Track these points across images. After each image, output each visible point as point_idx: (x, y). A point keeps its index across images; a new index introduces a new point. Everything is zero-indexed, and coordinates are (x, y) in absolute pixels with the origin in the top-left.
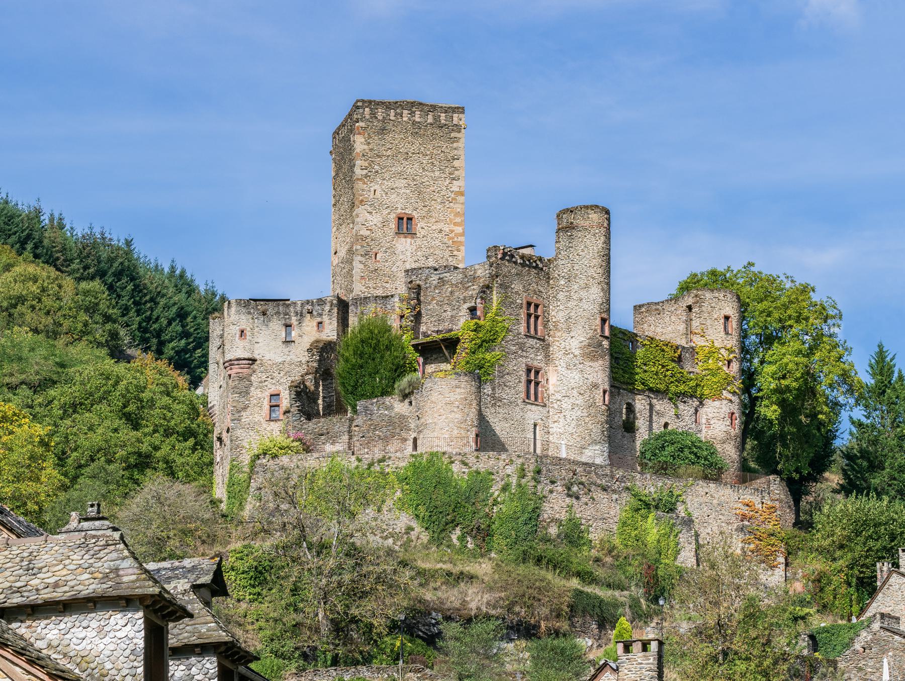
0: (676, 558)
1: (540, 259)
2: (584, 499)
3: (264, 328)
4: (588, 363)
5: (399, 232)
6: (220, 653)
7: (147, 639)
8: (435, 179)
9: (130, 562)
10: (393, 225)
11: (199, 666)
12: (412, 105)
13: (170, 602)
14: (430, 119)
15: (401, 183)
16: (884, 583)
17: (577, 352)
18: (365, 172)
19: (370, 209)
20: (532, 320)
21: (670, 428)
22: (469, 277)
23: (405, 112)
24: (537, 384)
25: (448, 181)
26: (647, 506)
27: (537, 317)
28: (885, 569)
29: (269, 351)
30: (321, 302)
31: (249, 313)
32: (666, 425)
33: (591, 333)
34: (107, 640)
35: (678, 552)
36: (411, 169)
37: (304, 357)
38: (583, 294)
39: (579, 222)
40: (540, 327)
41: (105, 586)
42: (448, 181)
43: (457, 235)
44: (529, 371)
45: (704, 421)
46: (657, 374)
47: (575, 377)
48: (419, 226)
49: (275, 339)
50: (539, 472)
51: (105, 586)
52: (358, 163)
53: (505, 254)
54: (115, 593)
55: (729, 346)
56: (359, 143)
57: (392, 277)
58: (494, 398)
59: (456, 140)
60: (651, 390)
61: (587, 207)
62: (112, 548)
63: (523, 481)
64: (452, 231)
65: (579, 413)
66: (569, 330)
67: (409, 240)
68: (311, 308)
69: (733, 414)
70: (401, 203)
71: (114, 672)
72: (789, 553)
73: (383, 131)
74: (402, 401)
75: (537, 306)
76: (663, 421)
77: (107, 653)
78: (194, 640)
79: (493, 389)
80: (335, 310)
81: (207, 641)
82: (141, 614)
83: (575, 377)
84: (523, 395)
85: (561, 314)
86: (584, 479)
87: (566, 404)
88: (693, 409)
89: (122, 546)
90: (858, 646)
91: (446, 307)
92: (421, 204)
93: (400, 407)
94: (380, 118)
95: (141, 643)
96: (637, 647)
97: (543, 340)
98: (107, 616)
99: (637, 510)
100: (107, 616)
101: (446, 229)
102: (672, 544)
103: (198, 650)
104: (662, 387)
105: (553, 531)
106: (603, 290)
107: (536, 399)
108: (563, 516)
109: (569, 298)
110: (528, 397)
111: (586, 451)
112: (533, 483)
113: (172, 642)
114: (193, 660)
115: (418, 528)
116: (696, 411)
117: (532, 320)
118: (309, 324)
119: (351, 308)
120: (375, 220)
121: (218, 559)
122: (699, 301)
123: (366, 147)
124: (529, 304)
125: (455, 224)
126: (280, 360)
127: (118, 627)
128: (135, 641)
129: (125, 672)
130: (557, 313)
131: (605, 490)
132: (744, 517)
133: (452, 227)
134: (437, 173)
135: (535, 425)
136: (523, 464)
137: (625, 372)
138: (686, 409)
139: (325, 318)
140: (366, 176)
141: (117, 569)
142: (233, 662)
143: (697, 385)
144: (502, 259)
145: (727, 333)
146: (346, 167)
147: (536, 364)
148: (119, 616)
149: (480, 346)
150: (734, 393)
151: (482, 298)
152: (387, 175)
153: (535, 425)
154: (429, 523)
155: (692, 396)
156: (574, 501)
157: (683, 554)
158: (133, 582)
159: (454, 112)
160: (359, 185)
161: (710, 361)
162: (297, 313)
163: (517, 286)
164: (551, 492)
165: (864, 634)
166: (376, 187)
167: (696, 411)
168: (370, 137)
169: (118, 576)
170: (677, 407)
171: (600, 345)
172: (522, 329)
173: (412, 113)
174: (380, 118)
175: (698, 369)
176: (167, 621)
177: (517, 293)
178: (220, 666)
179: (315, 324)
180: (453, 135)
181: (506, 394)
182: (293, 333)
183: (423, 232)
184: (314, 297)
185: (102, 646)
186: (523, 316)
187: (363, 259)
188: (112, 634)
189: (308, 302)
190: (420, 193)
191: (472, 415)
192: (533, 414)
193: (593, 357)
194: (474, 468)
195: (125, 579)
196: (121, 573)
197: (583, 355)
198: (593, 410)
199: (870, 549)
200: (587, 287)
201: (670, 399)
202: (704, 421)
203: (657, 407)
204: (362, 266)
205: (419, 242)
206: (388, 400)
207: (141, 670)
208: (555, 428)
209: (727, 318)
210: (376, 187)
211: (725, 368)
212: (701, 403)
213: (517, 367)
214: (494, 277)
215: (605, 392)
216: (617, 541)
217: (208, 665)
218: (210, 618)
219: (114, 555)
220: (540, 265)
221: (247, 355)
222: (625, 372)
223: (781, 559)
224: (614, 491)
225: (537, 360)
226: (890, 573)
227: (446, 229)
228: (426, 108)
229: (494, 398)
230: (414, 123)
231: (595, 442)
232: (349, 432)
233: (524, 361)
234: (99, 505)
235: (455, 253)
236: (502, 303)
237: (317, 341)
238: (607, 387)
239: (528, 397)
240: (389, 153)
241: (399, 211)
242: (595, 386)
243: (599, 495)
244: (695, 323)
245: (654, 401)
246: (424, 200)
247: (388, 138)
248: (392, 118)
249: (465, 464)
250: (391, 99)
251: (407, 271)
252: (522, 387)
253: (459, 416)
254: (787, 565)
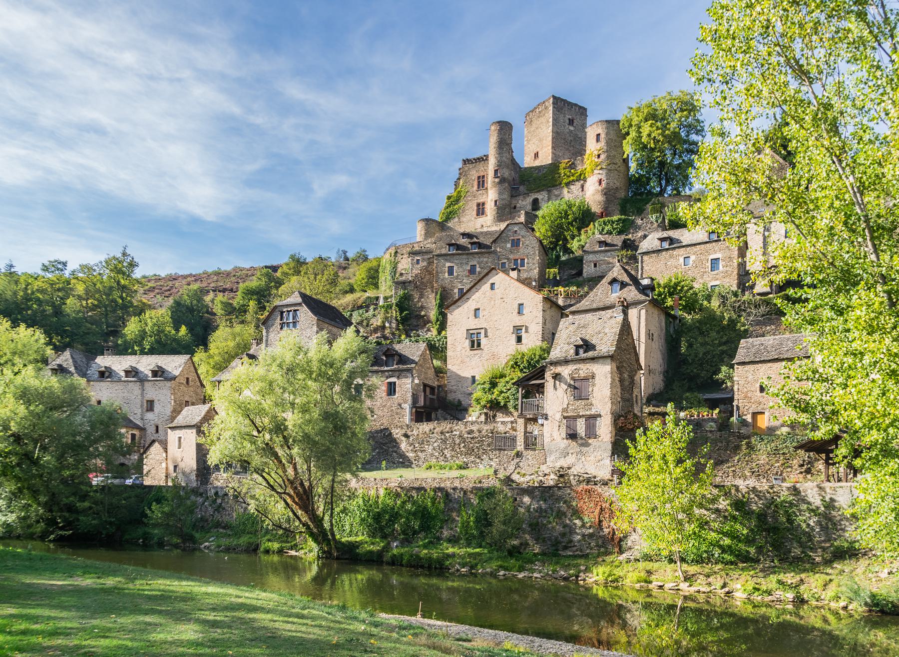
24: (483, 209)
27: (483, 181)
44: (478, 205)
55: (599, 148)
69: (601, 180)
75: (483, 177)
110: (477, 215)
116: (582, 187)
124: (479, 177)
138: (575, 188)
143: (581, 175)
150: (601, 169)
155: (577, 180)
186: (476, 183)
209: (598, 135)
211: (596, 160)
212: (585, 181)
214: (460, 174)
215: (496, 201)
236: (465, 182)
252: (475, 213)
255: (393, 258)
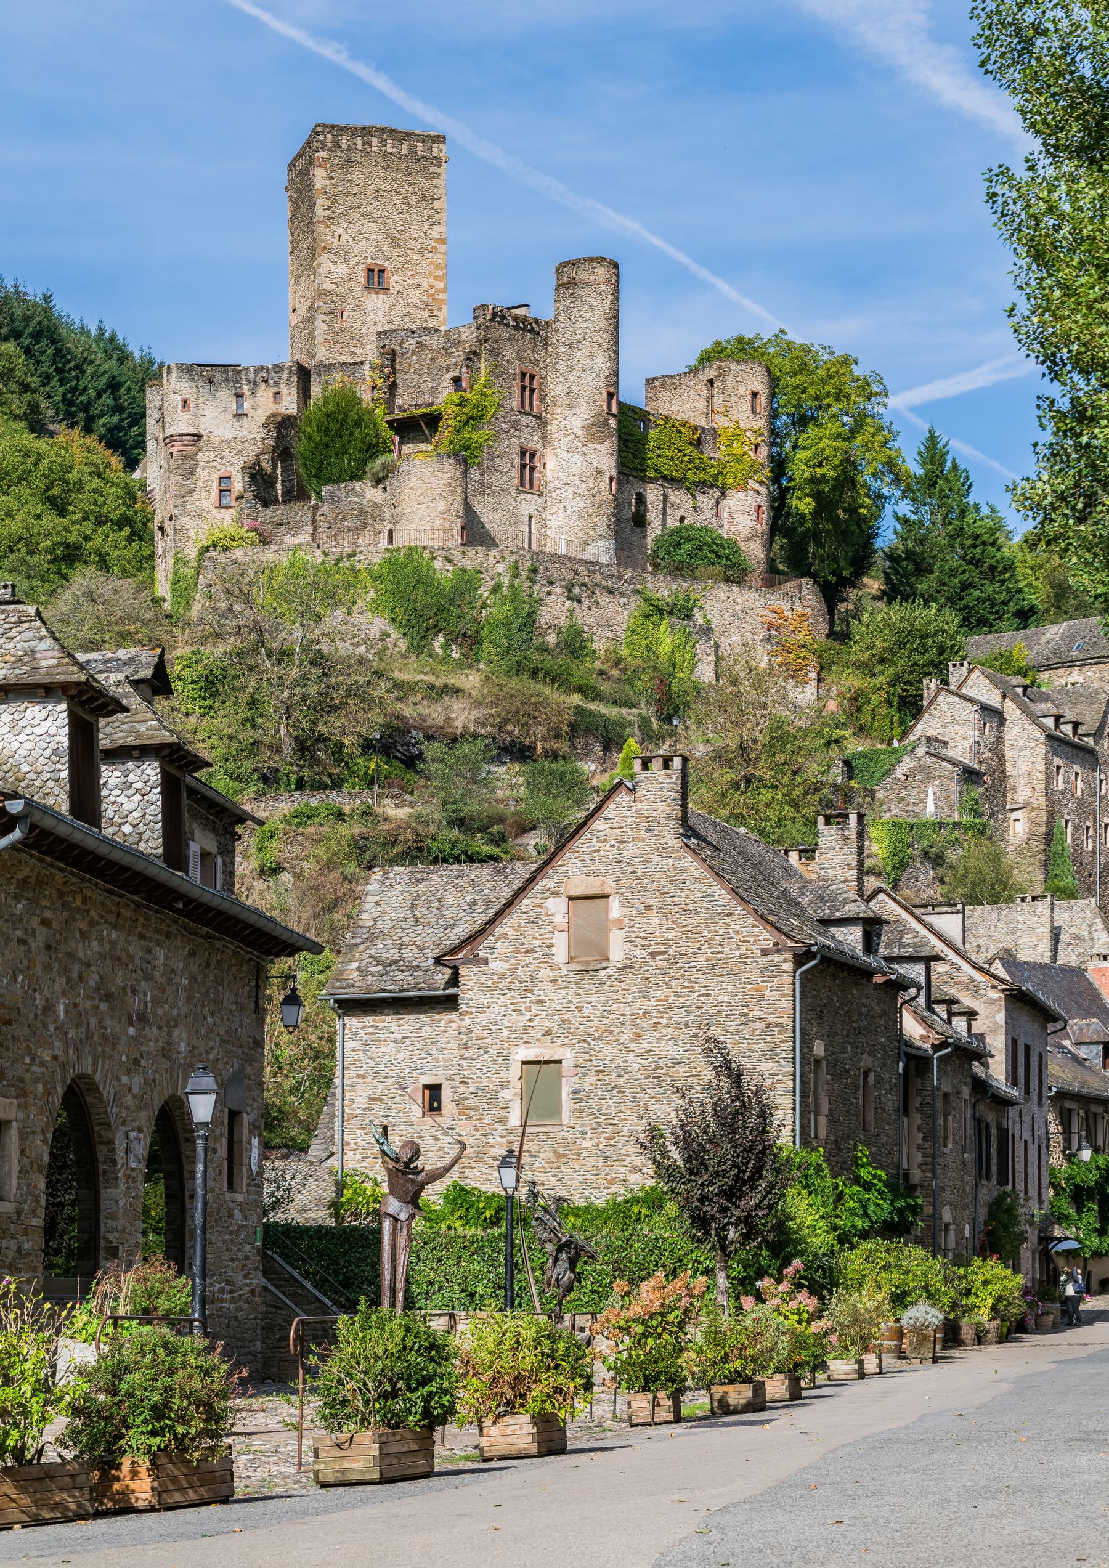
0: (692, 672)
1: (537, 321)
2: (587, 603)
3: (210, 398)
4: (592, 446)
5: (369, 287)
6: (164, 757)
7: (72, 736)
8: (411, 224)
9: (48, 643)
10: (362, 278)
11: (138, 772)
12: (383, 132)
13: (99, 692)
14: (405, 150)
15: (371, 227)
16: (931, 702)
17: (580, 432)
18: (327, 213)
19: (334, 258)
20: (527, 393)
21: (686, 522)
22: (453, 341)
23: (375, 140)
24: (532, 469)
25: (426, 226)
26: (660, 611)
27: (532, 391)
28: (933, 686)
29: (218, 425)
30: (278, 368)
31: (193, 380)
32: (682, 519)
33: (596, 410)
34: (22, 737)
35: (695, 665)
36: (383, 210)
37: (260, 435)
38: (587, 363)
39: (583, 277)
40: (536, 403)
41: (18, 672)
42: (426, 226)
43: (438, 291)
44: (523, 453)
45: (726, 515)
46: (672, 459)
47: (576, 462)
48: (393, 279)
49: (224, 412)
50: (535, 571)
51: (18, 672)
52: (319, 201)
53: (494, 315)
54: (30, 680)
55: (756, 428)
56: (320, 177)
57: (361, 340)
58: (482, 484)
59: (436, 176)
60: (665, 478)
61: (592, 260)
62: (27, 625)
63: (517, 581)
64: (432, 287)
65: (581, 503)
66: (570, 406)
67: (381, 296)
68: (267, 375)
70: (371, 251)
71: (32, 776)
72: (822, 668)
73: (348, 163)
74: (375, 486)
75: (532, 377)
76: (678, 514)
77: (24, 753)
78: (131, 741)
79: (482, 474)
80: (295, 378)
81: (146, 742)
82: (63, 706)
83: (576, 462)
84: (516, 482)
85: (561, 387)
86: (587, 580)
87: (567, 493)
88: (713, 502)
89: (38, 623)
90: (899, 774)
91: (425, 377)
92: (395, 253)
93: (373, 494)
94: (345, 147)
95: (65, 742)
96: (657, 764)
97: (540, 418)
98: (22, 708)
99: (649, 616)
100: (22, 708)
101: (425, 284)
102: (688, 656)
103: (136, 753)
104: (678, 475)
105: (551, 639)
106: (610, 358)
107: (531, 486)
108: (563, 622)
109: (570, 368)
110: (522, 484)
111: (589, 548)
112: (527, 584)
113: (104, 742)
114: (130, 765)
115: (394, 634)
116: (718, 503)
117: (527, 393)
118: (265, 395)
119: (314, 376)
120: (340, 271)
121: (159, 650)
122: (722, 374)
123: (328, 182)
124: (523, 375)
125: (436, 278)
126: (231, 436)
127: (36, 722)
128: (57, 738)
129: (45, 776)
130: (556, 387)
131: (611, 592)
132: (771, 626)
133: (432, 281)
134: (414, 216)
135: (530, 517)
136: (516, 562)
137: (635, 456)
138: (706, 501)
139: (283, 388)
140: (329, 218)
141: (33, 652)
142: (180, 768)
143: (719, 473)
144: (492, 320)
145: (754, 413)
146: (304, 207)
147: (531, 445)
148: (37, 708)
149: (466, 424)
150: (761, 483)
151: (468, 367)
152: (353, 218)
153: (530, 517)
154: (407, 627)
155: (712, 486)
156: (575, 604)
157: (700, 667)
158: (53, 667)
159: (433, 141)
160: (321, 229)
161: (735, 445)
162: (249, 382)
163: (509, 353)
164: (549, 594)
165: (906, 760)
166: (342, 231)
167: (718, 503)
168: (333, 170)
169: (34, 659)
170: (695, 498)
171: (607, 424)
172: (515, 404)
173: (383, 142)
174: (345, 147)
175: (720, 455)
176: (98, 716)
177: (509, 361)
178: (163, 772)
179: (271, 394)
180: (432, 170)
181: (496, 481)
182: (246, 405)
183: (397, 287)
184: (269, 362)
185: (16, 745)
186: (516, 389)
187: (327, 318)
188: (28, 730)
189: (262, 368)
190: (393, 240)
191: (456, 504)
192: (528, 504)
193: (598, 439)
194: (460, 565)
195: (43, 663)
196: (38, 656)
197: (587, 436)
198: (597, 501)
199: (915, 664)
200: (591, 355)
201: (688, 489)
202: (726, 515)
203: (672, 498)
204: (325, 327)
205: (392, 299)
206: (358, 485)
207: (65, 774)
208: (553, 521)
209: (755, 394)
210: (342, 231)
211: (752, 454)
212: (723, 494)
213: (509, 448)
215: (611, 479)
216: (624, 652)
217: (149, 771)
218: (150, 715)
219: (29, 634)
220: (537, 329)
221: (191, 430)
222: (635, 456)
223: (813, 675)
224: (622, 594)
225: (533, 441)
226: (938, 691)
227: (425, 284)
228: (400, 136)
229: (482, 484)
230: (386, 154)
231: (600, 538)
232: (314, 522)
233: (517, 441)
234: (13, 586)
235: (436, 313)
236: (492, 373)
237: (274, 415)
238: (614, 474)
239: (522, 484)
240: (356, 190)
241: (369, 261)
242: (600, 472)
243: (604, 598)
244: (718, 401)
245: (669, 491)
246: (398, 248)
247: (355, 171)
248: (359, 147)
249: (449, 561)
250: (360, 124)
251: (379, 334)
252: (515, 473)
253: (441, 505)
254: (819, 681)
255: (522, 582)
